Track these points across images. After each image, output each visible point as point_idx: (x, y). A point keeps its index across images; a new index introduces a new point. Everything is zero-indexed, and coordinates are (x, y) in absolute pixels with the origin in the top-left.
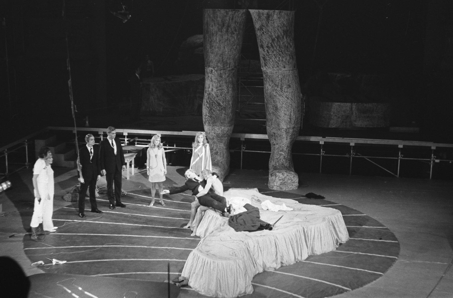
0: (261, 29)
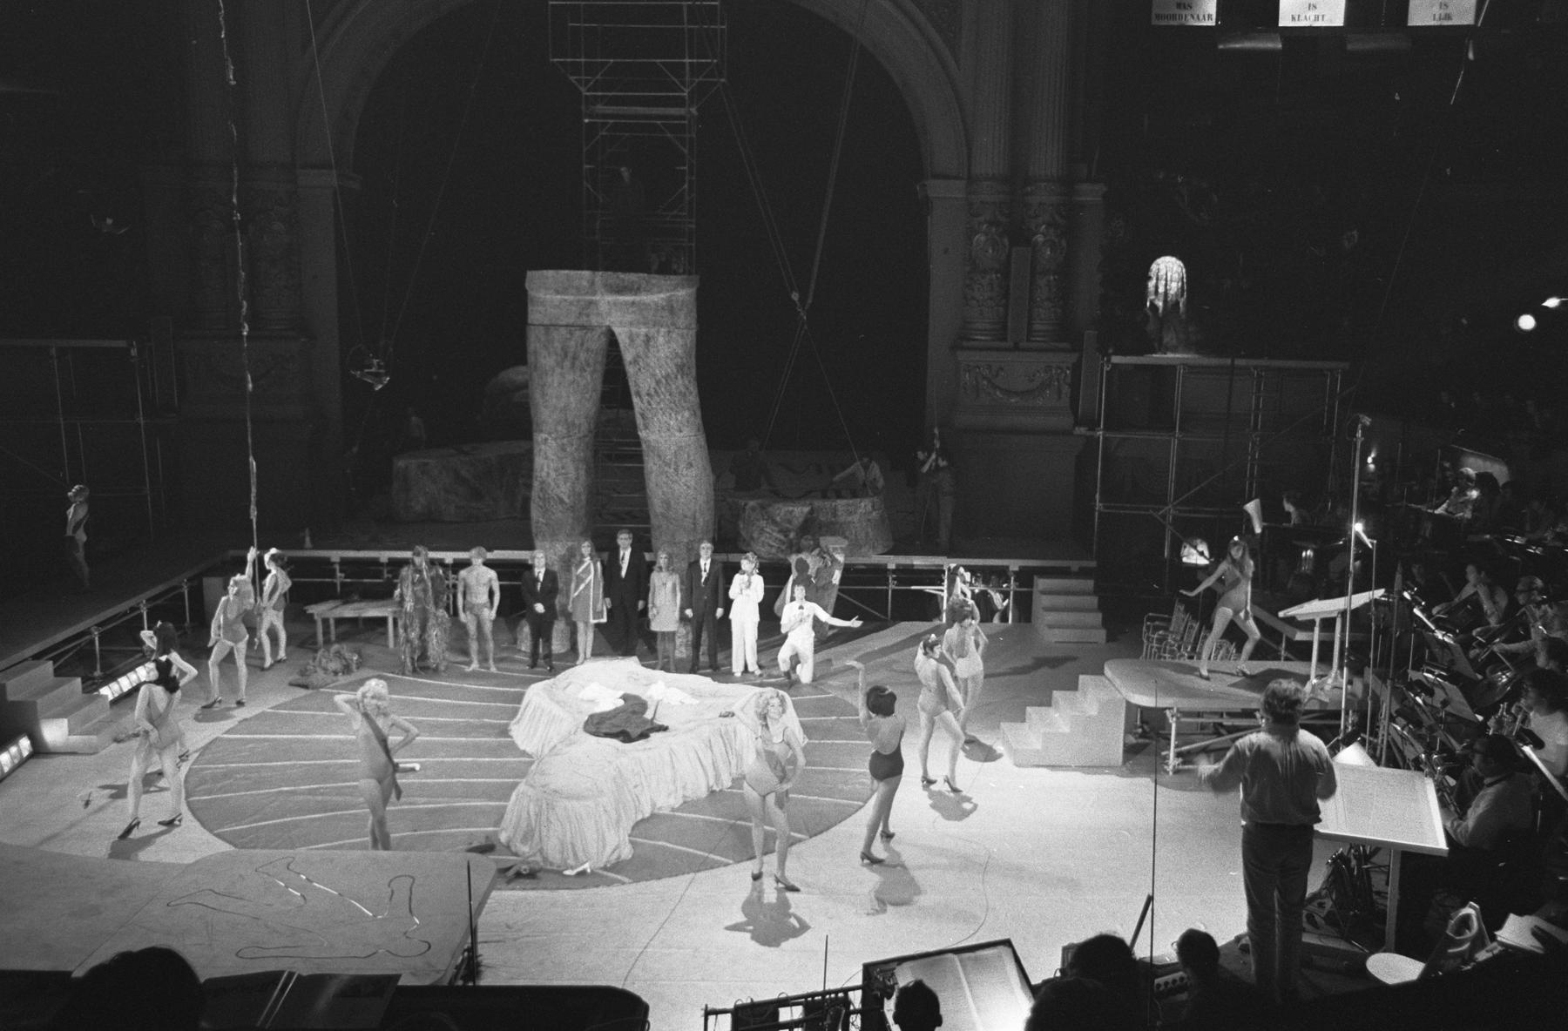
0: (635, 362)
